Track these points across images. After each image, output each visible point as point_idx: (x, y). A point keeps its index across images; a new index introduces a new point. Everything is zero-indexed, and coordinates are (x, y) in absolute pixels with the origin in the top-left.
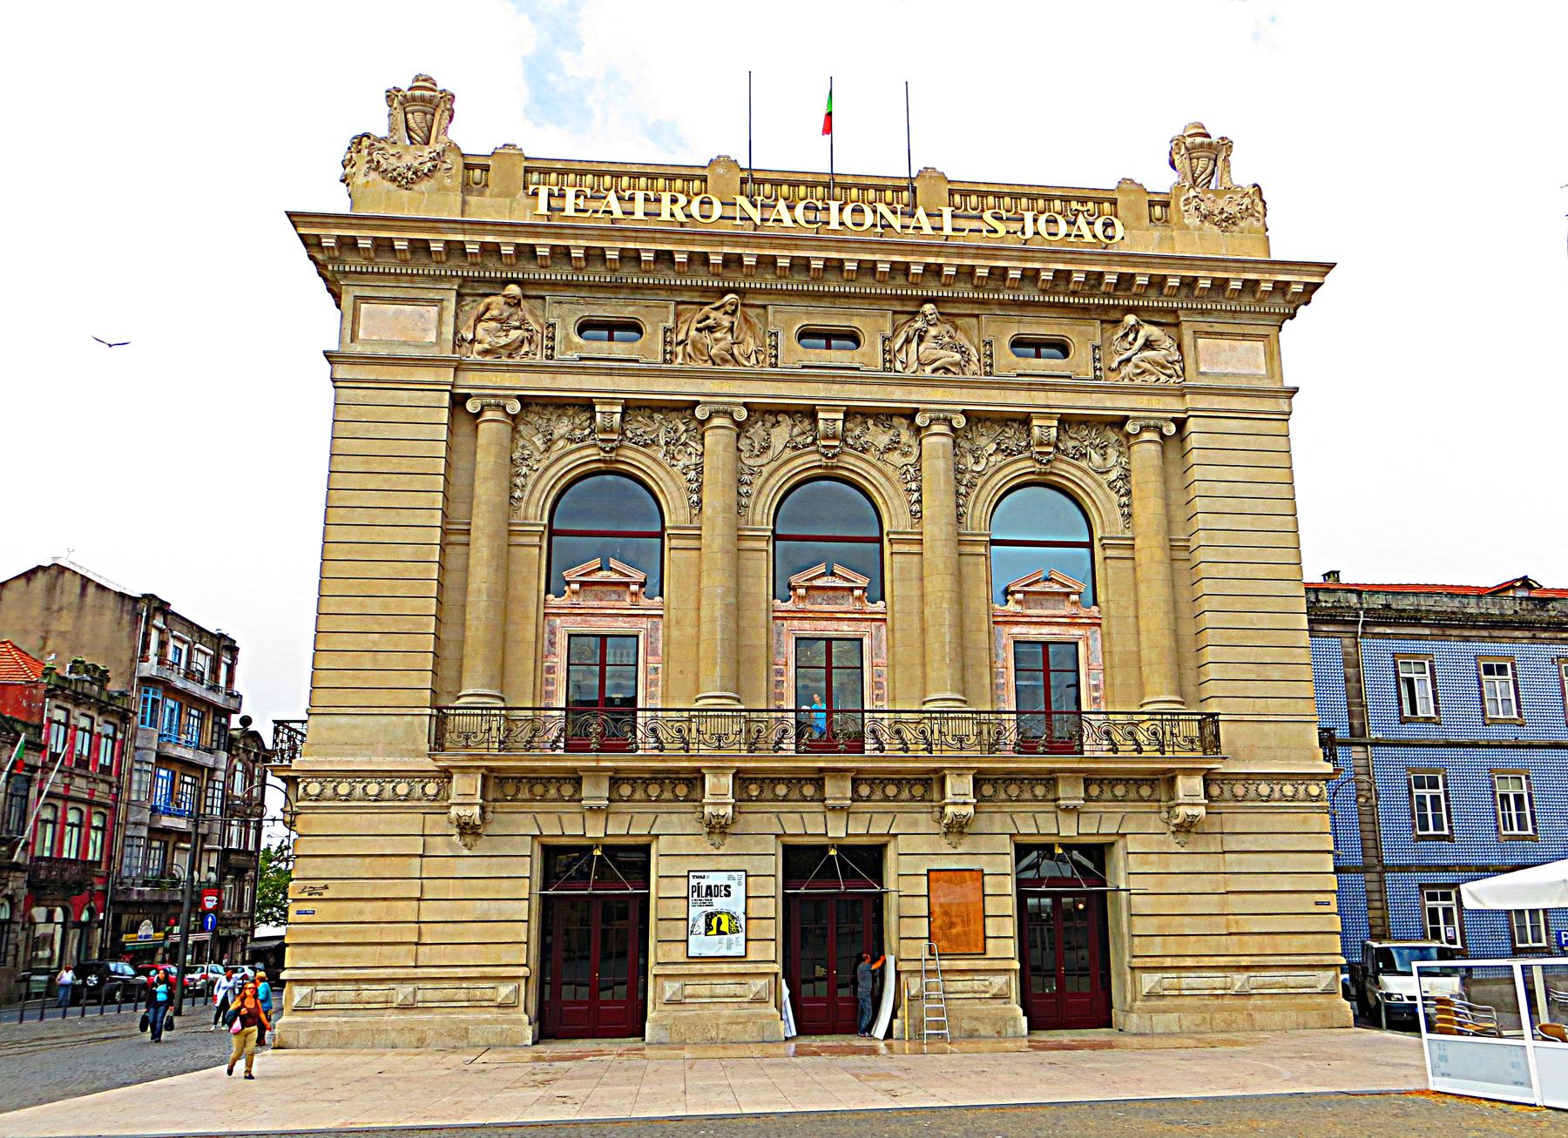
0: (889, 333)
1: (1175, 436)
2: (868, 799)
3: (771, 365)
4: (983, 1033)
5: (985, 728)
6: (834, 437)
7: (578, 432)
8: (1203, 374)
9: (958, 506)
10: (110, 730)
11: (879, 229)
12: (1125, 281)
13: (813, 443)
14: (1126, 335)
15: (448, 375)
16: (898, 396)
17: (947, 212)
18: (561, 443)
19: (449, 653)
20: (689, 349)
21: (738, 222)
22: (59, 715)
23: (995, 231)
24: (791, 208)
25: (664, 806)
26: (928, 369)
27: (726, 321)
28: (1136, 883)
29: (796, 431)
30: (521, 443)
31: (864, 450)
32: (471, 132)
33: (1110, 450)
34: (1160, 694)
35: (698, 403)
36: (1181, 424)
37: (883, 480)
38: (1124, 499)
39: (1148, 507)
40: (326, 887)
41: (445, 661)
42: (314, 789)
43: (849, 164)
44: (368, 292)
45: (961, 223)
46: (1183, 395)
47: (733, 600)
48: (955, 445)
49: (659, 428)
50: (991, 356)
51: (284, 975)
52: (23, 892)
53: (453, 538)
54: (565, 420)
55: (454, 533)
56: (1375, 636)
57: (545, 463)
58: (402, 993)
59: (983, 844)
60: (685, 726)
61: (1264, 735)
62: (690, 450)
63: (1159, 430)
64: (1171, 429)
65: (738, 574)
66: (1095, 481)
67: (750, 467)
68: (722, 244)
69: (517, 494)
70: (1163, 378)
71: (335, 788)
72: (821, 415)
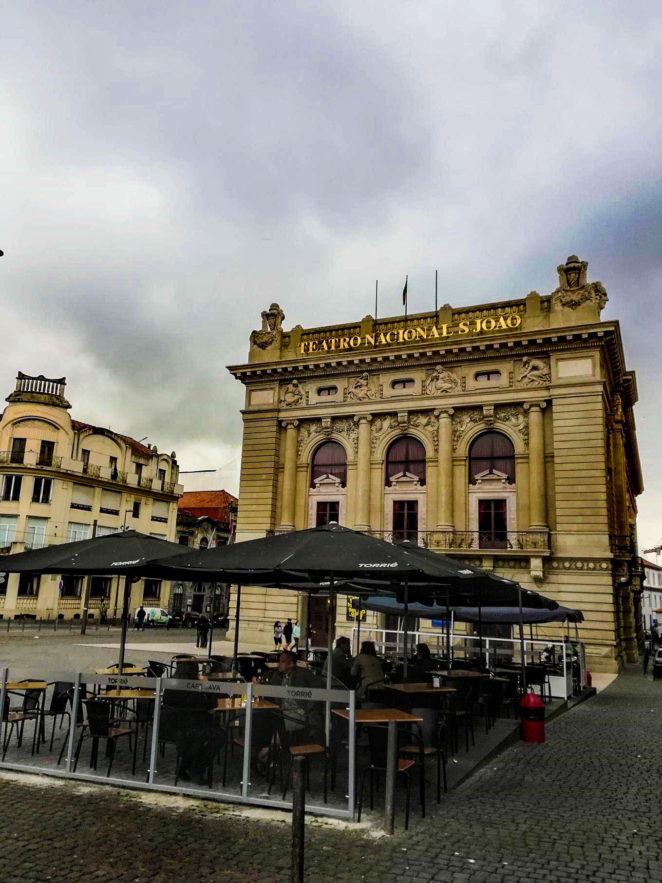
1: (547, 409)
6: (404, 423)
8: (560, 378)
15: (275, 414)
16: (426, 404)
17: (445, 326)
24: (385, 335)
27: (364, 382)
31: (417, 426)
32: (287, 326)
36: (549, 402)
43: (413, 310)
44: (254, 388)
48: (453, 420)
49: (344, 425)
58: (261, 626)
64: (544, 405)
65: (370, 478)
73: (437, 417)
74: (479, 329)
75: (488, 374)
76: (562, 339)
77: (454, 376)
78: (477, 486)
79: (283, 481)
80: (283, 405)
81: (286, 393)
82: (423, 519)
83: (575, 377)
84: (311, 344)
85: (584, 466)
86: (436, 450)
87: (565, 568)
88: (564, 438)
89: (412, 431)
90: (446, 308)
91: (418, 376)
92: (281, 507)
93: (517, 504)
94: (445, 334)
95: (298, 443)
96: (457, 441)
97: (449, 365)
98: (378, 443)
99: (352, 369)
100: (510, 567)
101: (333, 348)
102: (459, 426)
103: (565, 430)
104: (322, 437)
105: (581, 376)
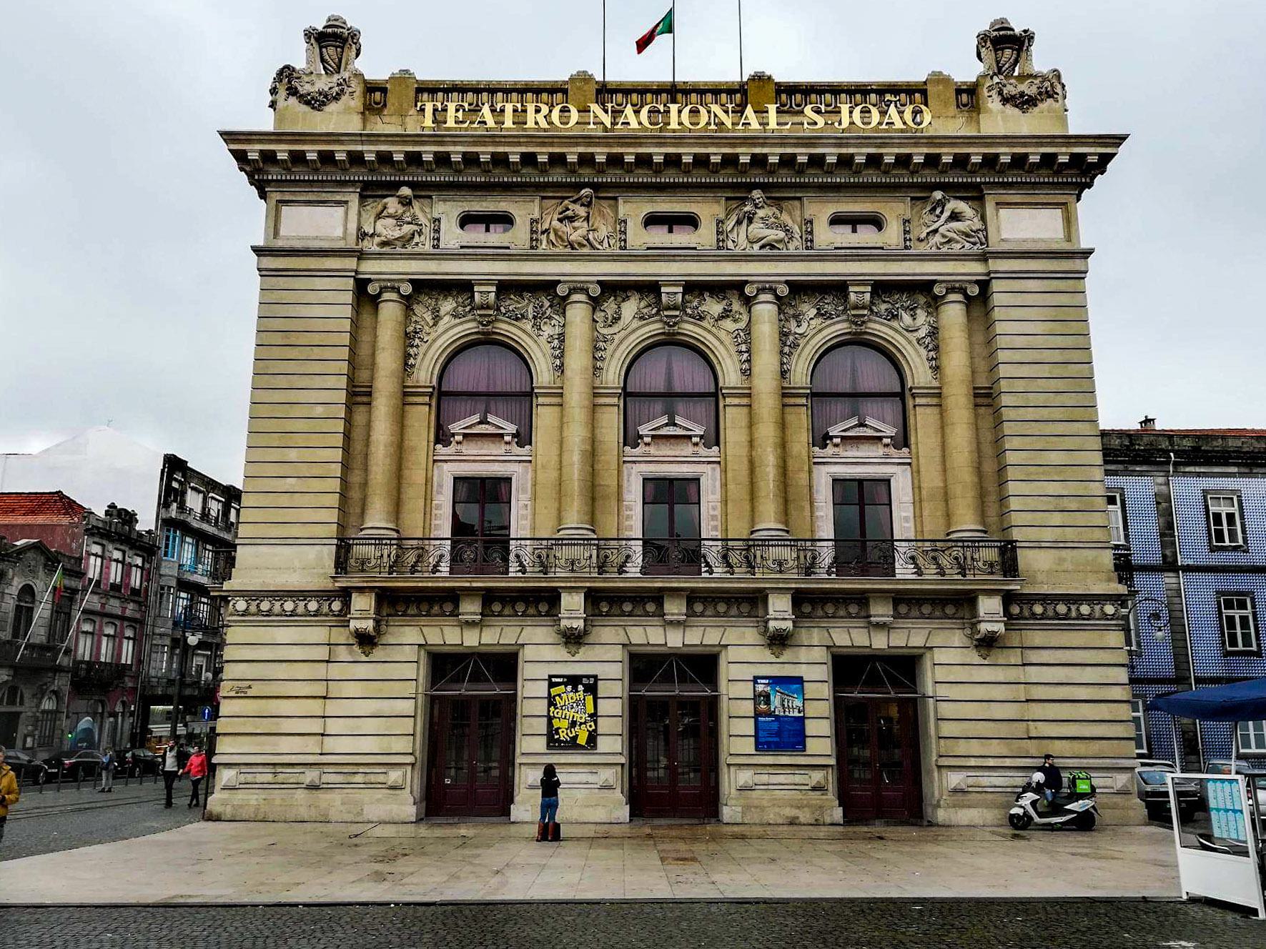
0: (722, 216)
1: (979, 300)
2: (702, 615)
3: (621, 248)
4: (802, 820)
5: (802, 554)
7: (460, 309)
9: (782, 364)
10: (139, 561)
11: (713, 127)
12: (932, 161)
13: (658, 313)
14: (934, 209)
15: (351, 263)
17: (772, 108)
18: (447, 319)
19: (355, 494)
20: (552, 237)
21: (592, 126)
22: (96, 549)
23: (816, 123)
24: (637, 112)
25: (529, 621)
26: (756, 247)
27: (582, 211)
28: (943, 691)
29: (643, 304)
30: (414, 318)
31: (701, 318)
32: (373, 63)
33: (919, 311)
34: (966, 523)
35: (559, 282)
36: (984, 285)
37: (717, 343)
38: (932, 353)
39: (957, 360)
40: (250, 687)
41: (350, 502)
42: (241, 605)
44: (287, 197)
45: (786, 118)
46: (986, 260)
47: (589, 448)
48: (780, 311)
50: (811, 233)
51: (215, 760)
52: (66, 689)
53: (359, 399)
54: (450, 299)
55: (359, 395)
56: (1185, 474)
57: (433, 336)
58: (310, 776)
59: (803, 654)
60: (544, 553)
61: (1061, 560)
62: (553, 322)
63: (963, 291)
64: (974, 291)
66: (903, 336)
67: (603, 336)
68: (577, 144)
69: (411, 361)
70: (967, 245)
71: (258, 606)
72: (663, 289)
73: (748, 302)
74: (845, 124)
75: (853, 221)
76: (1019, 161)
77: (785, 218)
78: (830, 450)
79: (369, 426)
80: (371, 246)
81: (379, 216)
82: (714, 518)
83: (1034, 241)
84: (452, 107)
85: (1057, 414)
86: (747, 373)
87: (1033, 616)
88: (1017, 356)
89: (689, 328)
90: (760, 79)
91: (708, 210)
92: (365, 484)
93: (917, 488)
94: (773, 124)
95: (409, 338)
96: (790, 354)
97: (778, 195)
98: (609, 352)
99: (557, 176)
100: (923, 616)
101: (508, 123)
102: (793, 325)
103: (1020, 341)
104: (471, 327)
105: (1043, 240)
